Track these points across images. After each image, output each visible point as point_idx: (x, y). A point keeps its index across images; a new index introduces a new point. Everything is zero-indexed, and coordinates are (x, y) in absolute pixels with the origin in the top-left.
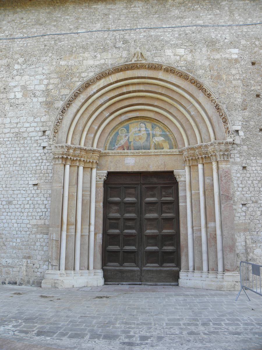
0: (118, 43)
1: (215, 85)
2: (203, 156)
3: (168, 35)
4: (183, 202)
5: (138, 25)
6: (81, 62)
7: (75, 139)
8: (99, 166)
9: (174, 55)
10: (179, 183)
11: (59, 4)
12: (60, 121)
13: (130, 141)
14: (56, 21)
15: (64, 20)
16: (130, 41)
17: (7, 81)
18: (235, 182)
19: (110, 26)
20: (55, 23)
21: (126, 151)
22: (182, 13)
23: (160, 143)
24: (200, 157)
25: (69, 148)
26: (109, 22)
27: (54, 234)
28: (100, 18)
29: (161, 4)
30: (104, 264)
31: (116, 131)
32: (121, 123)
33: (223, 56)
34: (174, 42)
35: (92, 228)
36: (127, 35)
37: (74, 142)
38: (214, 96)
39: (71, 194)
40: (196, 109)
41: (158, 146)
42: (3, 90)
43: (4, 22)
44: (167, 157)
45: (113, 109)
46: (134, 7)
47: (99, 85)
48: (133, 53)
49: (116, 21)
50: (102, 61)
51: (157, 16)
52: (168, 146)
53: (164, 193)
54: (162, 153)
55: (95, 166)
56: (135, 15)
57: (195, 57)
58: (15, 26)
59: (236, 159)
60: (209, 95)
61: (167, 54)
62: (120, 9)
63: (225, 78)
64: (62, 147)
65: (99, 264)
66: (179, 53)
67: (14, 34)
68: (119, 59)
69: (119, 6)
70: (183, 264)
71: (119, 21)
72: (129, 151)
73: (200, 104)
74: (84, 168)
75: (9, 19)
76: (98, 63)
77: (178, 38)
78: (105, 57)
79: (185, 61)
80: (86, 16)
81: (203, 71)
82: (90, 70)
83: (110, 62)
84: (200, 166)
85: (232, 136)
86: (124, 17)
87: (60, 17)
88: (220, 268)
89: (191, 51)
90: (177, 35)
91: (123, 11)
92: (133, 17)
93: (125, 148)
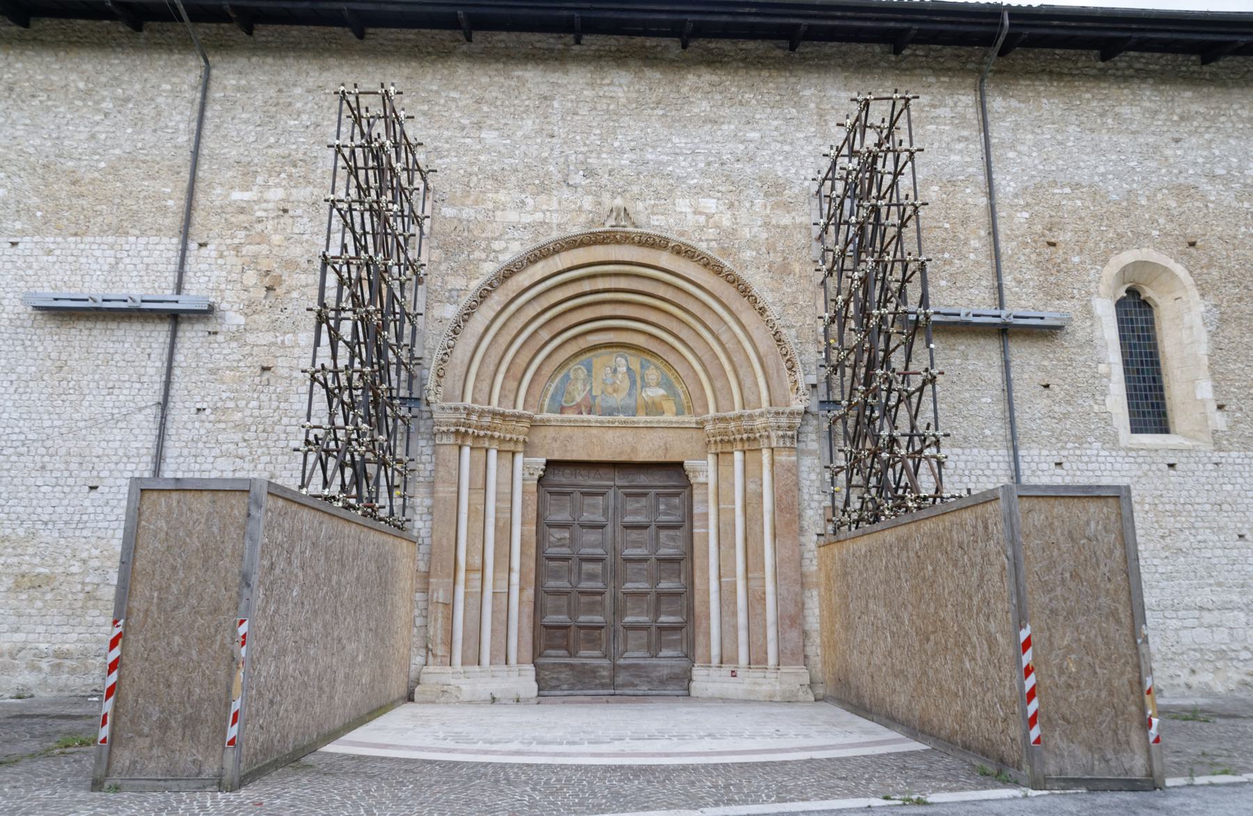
0: (572, 175)
1: (777, 285)
2: (745, 436)
3: (683, 164)
4: (702, 527)
5: (618, 131)
6: (491, 214)
7: (481, 390)
8: (528, 448)
10: (695, 486)
11: (434, 57)
12: (449, 351)
13: (594, 394)
15: (446, 101)
16: (600, 172)
17: (314, 243)
18: (805, 490)
19: (556, 128)
20: (426, 108)
21: (585, 416)
22: (715, 109)
23: (657, 400)
24: (738, 437)
25: (469, 412)
26: (553, 119)
27: (441, 591)
28: (532, 105)
29: (671, 82)
30: (537, 654)
31: (564, 372)
32: (576, 355)
33: (798, 220)
34: (696, 181)
35: (515, 578)
36: (594, 155)
37: (477, 397)
38: (773, 312)
39: (473, 508)
40: (735, 335)
41: (654, 408)
42: (305, 265)
43: (298, 91)
44: (671, 433)
45: (561, 324)
46: (609, 85)
47: (534, 274)
48: (608, 209)
50: (539, 216)
51: (661, 112)
52: (674, 409)
53: (662, 507)
54: (662, 425)
55: (520, 448)
56: (612, 107)
57: (738, 221)
58: (326, 104)
59: (810, 443)
60: (762, 311)
61: (678, 209)
62: (578, 88)
63: (797, 270)
64: (457, 409)
65: (528, 654)
66: (704, 207)
67: (325, 123)
68: (574, 214)
69: (575, 79)
70: (700, 651)
71: (577, 118)
72: (592, 417)
73: (743, 327)
74: (498, 451)
75: (311, 82)
76: (527, 219)
77: (703, 173)
78: (545, 207)
80: (500, 96)
81: (754, 253)
83: (555, 219)
84: (738, 456)
85: (803, 398)
86: (587, 109)
87: (437, 92)
88: (772, 659)
89: (731, 206)
90: (702, 165)
91: (585, 92)
92: (608, 111)
93: (583, 409)
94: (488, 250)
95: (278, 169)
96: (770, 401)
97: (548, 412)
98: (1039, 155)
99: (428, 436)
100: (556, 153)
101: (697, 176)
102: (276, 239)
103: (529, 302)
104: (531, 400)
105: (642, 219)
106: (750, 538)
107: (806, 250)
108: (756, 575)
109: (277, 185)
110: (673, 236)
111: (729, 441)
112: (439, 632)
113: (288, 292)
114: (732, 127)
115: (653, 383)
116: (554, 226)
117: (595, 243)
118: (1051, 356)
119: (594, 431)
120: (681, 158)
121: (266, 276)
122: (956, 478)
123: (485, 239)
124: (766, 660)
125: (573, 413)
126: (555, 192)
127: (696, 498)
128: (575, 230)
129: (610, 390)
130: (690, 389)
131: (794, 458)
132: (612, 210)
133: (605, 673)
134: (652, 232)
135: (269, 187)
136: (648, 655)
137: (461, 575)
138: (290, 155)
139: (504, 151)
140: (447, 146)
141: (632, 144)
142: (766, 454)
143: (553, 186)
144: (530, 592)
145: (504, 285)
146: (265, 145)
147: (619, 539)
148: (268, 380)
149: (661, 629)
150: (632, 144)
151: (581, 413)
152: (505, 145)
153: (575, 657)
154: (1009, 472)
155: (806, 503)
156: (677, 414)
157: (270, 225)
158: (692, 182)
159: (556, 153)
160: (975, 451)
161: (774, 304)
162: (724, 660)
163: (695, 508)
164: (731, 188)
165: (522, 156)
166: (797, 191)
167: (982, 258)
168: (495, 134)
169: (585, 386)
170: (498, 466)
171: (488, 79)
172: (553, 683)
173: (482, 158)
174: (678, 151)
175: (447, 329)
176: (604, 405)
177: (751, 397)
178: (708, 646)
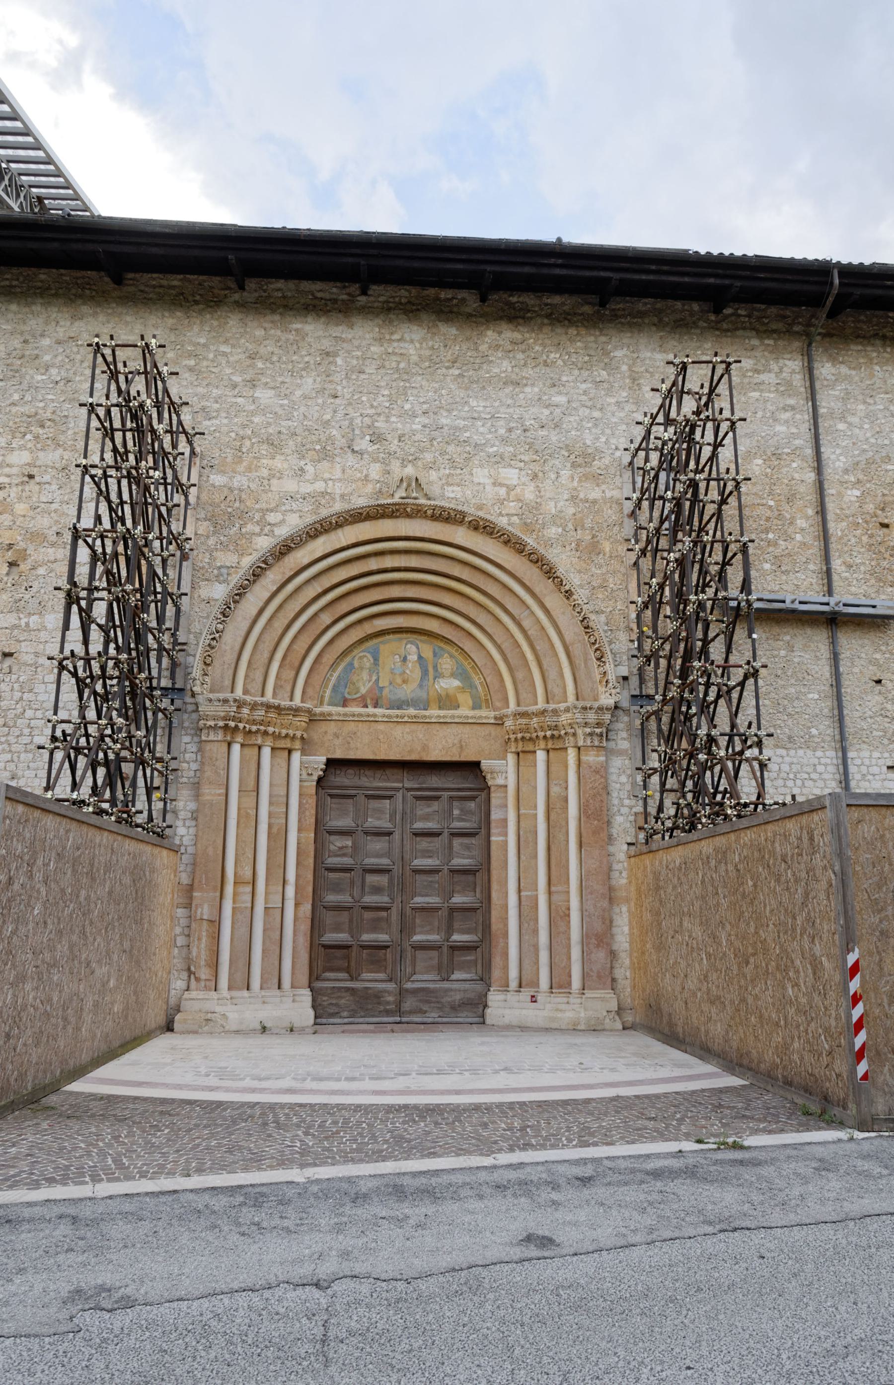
0: (358, 440)
2: (549, 733)
3: (481, 429)
4: (500, 835)
5: (409, 392)
6: (266, 482)
7: (253, 680)
8: (307, 746)
9: (494, 484)
10: (492, 789)
11: (201, 306)
13: (381, 685)
14: (190, 355)
16: (389, 437)
17: (63, 514)
18: (615, 794)
19: (339, 388)
20: (192, 363)
21: (371, 710)
22: (516, 370)
23: (451, 692)
24: (541, 734)
25: (240, 704)
26: (337, 378)
27: (206, 906)
29: (468, 339)
30: (314, 977)
31: (348, 659)
32: (361, 641)
33: (609, 494)
34: (495, 449)
35: (290, 891)
36: (382, 418)
37: (249, 687)
38: (581, 595)
40: (538, 621)
41: (447, 701)
42: (54, 538)
43: (46, 342)
45: (345, 606)
46: (399, 340)
48: (397, 478)
49: (354, 377)
50: (320, 486)
51: (457, 372)
52: (470, 703)
53: (456, 812)
54: (457, 720)
55: (297, 745)
56: (402, 365)
57: (542, 493)
58: (79, 357)
59: (620, 742)
60: (569, 594)
61: (476, 480)
62: (364, 343)
63: (607, 549)
64: (226, 701)
65: (304, 979)
66: (505, 478)
67: (78, 378)
69: (360, 333)
70: (496, 973)
71: (363, 376)
72: (379, 711)
74: (273, 749)
75: (61, 333)
76: (307, 488)
77: (504, 440)
79: (519, 500)
80: (277, 351)
81: (560, 530)
82: (288, 507)
83: (338, 489)
84: (541, 755)
85: (613, 691)
86: (374, 367)
87: (204, 345)
88: (576, 983)
89: (535, 477)
91: (372, 348)
92: (397, 370)
93: (369, 701)
94: (262, 523)
95: (22, 429)
96: (577, 694)
97: (329, 705)
98: (872, 428)
99: (193, 732)
100: (340, 415)
101: (497, 443)
102: (21, 508)
103: (308, 581)
104: (310, 691)
105: (435, 490)
106: (553, 847)
107: (617, 528)
108: (560, 888)
109: (21, 448)
110: (471, 510)
111: (531, 739)
112: (203, 952)
113: (34, 568)
114: (536, 390)
115: (447, 673)
116: (337, 497)
117: (383, 516)
118: (883, 648)
119: (381, 727)
120: (479, 423)
121: (8, 550)
122: (780, 782)
123: (258, 511)
124: (569, 984)
125: (357, 706)
126: (338, 459)
127: (494, 802)
128: (360, 502)
129: (399, 680)
130: (488, 680)
131: (603, 759)
132: (402, 480)
133: (391, 999)
134: (447, 505)
135: (13, 450)
136: (438, 978)
137: (229, 889)
138: (36, 414)
139: (280, 412)
140: (216, 406)
141: (425, 406)
142: (572, 754)
143: (336, 452)
144: (307, 908)
145: (281, 563)
146: (8, 402)
147: (407, 847)
148: (10, 667)
149: (453, 948)
150: (425, 406)
151: (366, 706)
152: (282, 405)
153: (357, 980)
154: (837, 776)
155: (616, 809)
156: (474, 708)
157: (14, 492)
158: (491, 450)
159: (340, 415)
160: (801, 752)
161: (581, 586)
162: (524, 983)
163: (492, 813)
164: (535, 457)
165: (301, 417)
166: (607, 462)
167: (809, 539)
168: (271, 393)
169: (371, 676)
170: (272, 765)
171: (263, 332)
172: (332, 1010)
173: (256, 420)
174: (476, 415)
175: (216, 610)
176: (393, 698)
177: (557, 691)
178: (506, 968)
